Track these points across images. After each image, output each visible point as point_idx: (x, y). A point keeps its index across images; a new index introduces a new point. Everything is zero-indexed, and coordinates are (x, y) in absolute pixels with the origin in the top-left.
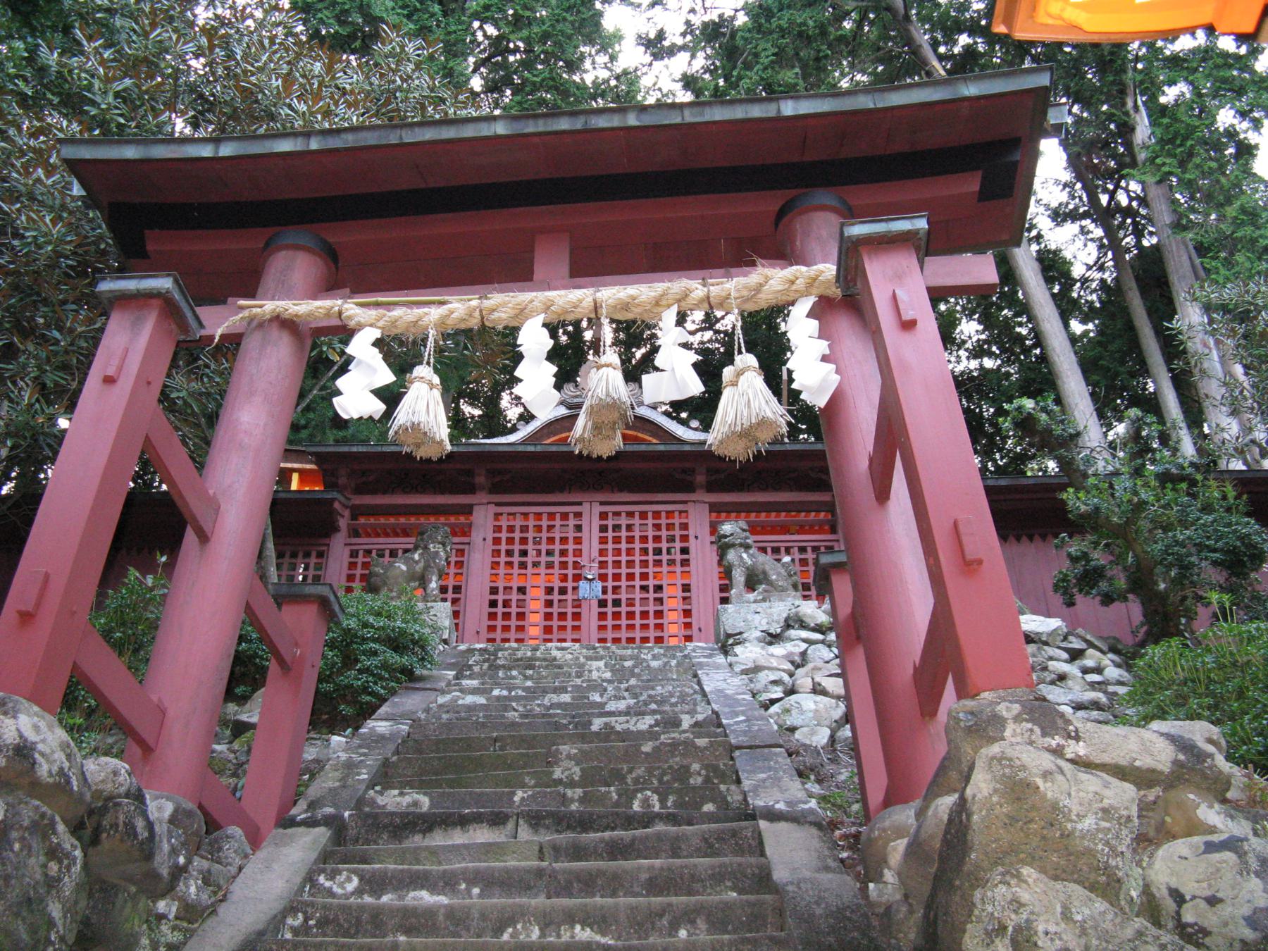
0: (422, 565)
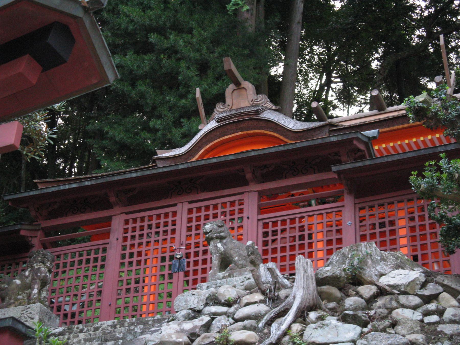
0: (30, 278)
